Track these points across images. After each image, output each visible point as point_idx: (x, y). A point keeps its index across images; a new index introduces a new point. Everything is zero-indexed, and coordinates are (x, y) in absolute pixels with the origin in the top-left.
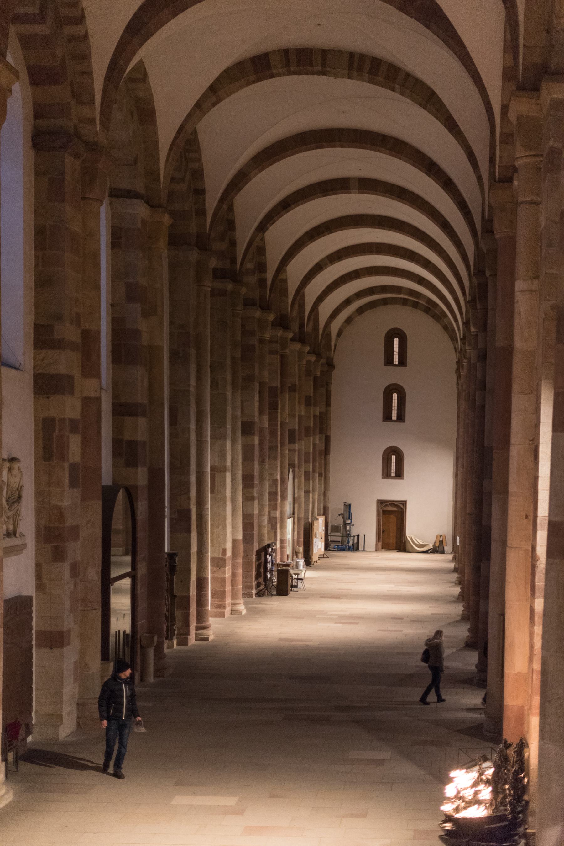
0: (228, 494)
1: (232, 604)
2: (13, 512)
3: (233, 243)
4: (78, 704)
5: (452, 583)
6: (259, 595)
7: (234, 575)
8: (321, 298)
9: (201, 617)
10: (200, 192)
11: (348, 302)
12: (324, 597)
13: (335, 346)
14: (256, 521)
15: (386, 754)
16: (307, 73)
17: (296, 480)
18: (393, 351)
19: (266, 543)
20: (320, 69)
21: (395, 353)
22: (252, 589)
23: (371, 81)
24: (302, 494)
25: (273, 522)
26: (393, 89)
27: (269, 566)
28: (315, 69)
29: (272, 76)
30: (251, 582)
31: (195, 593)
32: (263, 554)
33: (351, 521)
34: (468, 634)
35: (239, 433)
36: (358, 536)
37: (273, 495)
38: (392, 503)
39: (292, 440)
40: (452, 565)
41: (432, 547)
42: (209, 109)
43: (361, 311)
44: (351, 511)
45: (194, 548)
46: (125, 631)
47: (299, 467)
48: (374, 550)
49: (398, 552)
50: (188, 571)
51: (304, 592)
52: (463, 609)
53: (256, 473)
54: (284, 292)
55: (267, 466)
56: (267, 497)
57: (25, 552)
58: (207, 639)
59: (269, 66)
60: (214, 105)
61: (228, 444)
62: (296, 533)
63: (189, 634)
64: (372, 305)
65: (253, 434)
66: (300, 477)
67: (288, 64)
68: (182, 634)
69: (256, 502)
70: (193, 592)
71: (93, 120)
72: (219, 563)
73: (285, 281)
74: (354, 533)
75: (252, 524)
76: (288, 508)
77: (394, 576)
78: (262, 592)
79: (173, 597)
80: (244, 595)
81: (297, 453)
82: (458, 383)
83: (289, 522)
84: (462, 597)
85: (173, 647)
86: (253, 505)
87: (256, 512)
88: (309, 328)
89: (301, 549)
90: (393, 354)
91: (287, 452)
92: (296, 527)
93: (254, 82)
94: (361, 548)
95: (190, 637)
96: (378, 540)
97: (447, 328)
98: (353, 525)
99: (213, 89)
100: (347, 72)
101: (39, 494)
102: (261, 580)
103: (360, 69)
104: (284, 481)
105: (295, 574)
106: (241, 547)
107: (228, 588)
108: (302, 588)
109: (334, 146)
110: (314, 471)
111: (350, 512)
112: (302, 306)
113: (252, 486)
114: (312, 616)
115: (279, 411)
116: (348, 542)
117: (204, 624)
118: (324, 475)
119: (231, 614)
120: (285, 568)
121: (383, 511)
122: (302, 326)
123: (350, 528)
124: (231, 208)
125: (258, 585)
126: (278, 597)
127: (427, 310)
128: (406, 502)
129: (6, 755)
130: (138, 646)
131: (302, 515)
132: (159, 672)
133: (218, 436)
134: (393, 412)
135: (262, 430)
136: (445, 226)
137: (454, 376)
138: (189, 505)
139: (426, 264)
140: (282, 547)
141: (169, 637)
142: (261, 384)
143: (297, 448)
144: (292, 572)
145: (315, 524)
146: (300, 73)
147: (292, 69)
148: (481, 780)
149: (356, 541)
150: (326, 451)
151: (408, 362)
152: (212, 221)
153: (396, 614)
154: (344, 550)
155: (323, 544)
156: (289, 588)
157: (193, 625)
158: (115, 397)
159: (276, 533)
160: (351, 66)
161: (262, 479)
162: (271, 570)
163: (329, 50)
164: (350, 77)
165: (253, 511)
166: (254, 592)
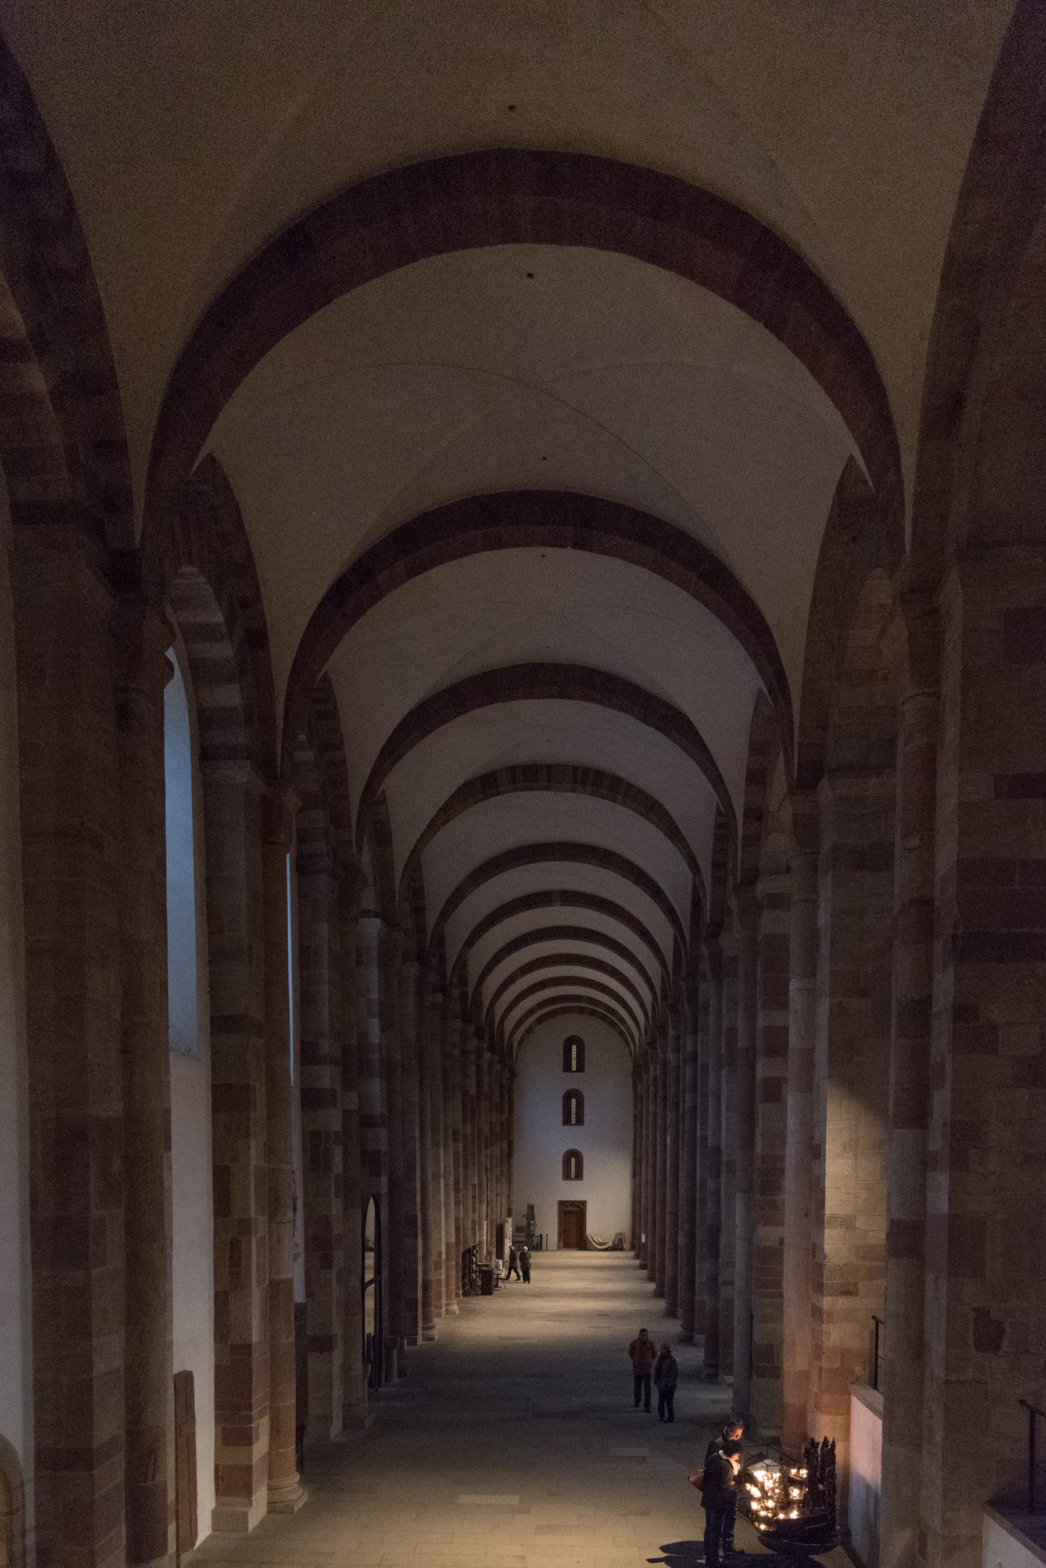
0: (442, 1199)
3: (443, 959)
4: (343, 1406)
6: (465, 1294)
8: (510, 1009)
9: (427, 1318)
11: (531, 1012)
13: (517, 1054)
15: (645, 1452)
19: (471, 1245)
20: (544, 784)
23: (594, 794)
24: (494, 1197)
26: (615, 801)
29: (498, 794)
35: (450, 1141)
36: (541, 1235)
38: (573, 1203)
43: (540, 1020)
47: (491, 1171)
49: (579, 1250)
56: (470, 1201)
58: (433, 1339)
60: (444, 824)
62: (489, 1234)
70: (420, 1295)
72: (438, 1266)
74: (537, 1233)
77: (584, 1273)
82: (635, 1087)
84: (659, 1294)
90: (571, 1061)
91: (483, 1158)
95: (418, 1337)
96: (559, 1240)
98: (536, 1226)
99: (444, 809)
100: (570, 785)
101: (306, 1204)
102: (467, 1281)
106: (453, 1250)
107: (444, 1289)
108: (503, 1287)
114: (522, 1314)
116: (532, 1242)
122: (492, 1036)
123: (534, 1228)
125: (464, 1285)
127: (604, 1018)
130: (383, 1348)
132: (402, 1373)
133: (436, 1144)
134: (572, 1116)
135: (465, 1137)
136: (644, 934)
138: (415, 1209)
139: (613, 972)
142: (465, 1093)
145: (506, 1226)
150: (510, 1156)
151: (586, 1066)
157: (420, 1325)
163: (555, 765)
164: (573, 791)
166: (461, 1292)
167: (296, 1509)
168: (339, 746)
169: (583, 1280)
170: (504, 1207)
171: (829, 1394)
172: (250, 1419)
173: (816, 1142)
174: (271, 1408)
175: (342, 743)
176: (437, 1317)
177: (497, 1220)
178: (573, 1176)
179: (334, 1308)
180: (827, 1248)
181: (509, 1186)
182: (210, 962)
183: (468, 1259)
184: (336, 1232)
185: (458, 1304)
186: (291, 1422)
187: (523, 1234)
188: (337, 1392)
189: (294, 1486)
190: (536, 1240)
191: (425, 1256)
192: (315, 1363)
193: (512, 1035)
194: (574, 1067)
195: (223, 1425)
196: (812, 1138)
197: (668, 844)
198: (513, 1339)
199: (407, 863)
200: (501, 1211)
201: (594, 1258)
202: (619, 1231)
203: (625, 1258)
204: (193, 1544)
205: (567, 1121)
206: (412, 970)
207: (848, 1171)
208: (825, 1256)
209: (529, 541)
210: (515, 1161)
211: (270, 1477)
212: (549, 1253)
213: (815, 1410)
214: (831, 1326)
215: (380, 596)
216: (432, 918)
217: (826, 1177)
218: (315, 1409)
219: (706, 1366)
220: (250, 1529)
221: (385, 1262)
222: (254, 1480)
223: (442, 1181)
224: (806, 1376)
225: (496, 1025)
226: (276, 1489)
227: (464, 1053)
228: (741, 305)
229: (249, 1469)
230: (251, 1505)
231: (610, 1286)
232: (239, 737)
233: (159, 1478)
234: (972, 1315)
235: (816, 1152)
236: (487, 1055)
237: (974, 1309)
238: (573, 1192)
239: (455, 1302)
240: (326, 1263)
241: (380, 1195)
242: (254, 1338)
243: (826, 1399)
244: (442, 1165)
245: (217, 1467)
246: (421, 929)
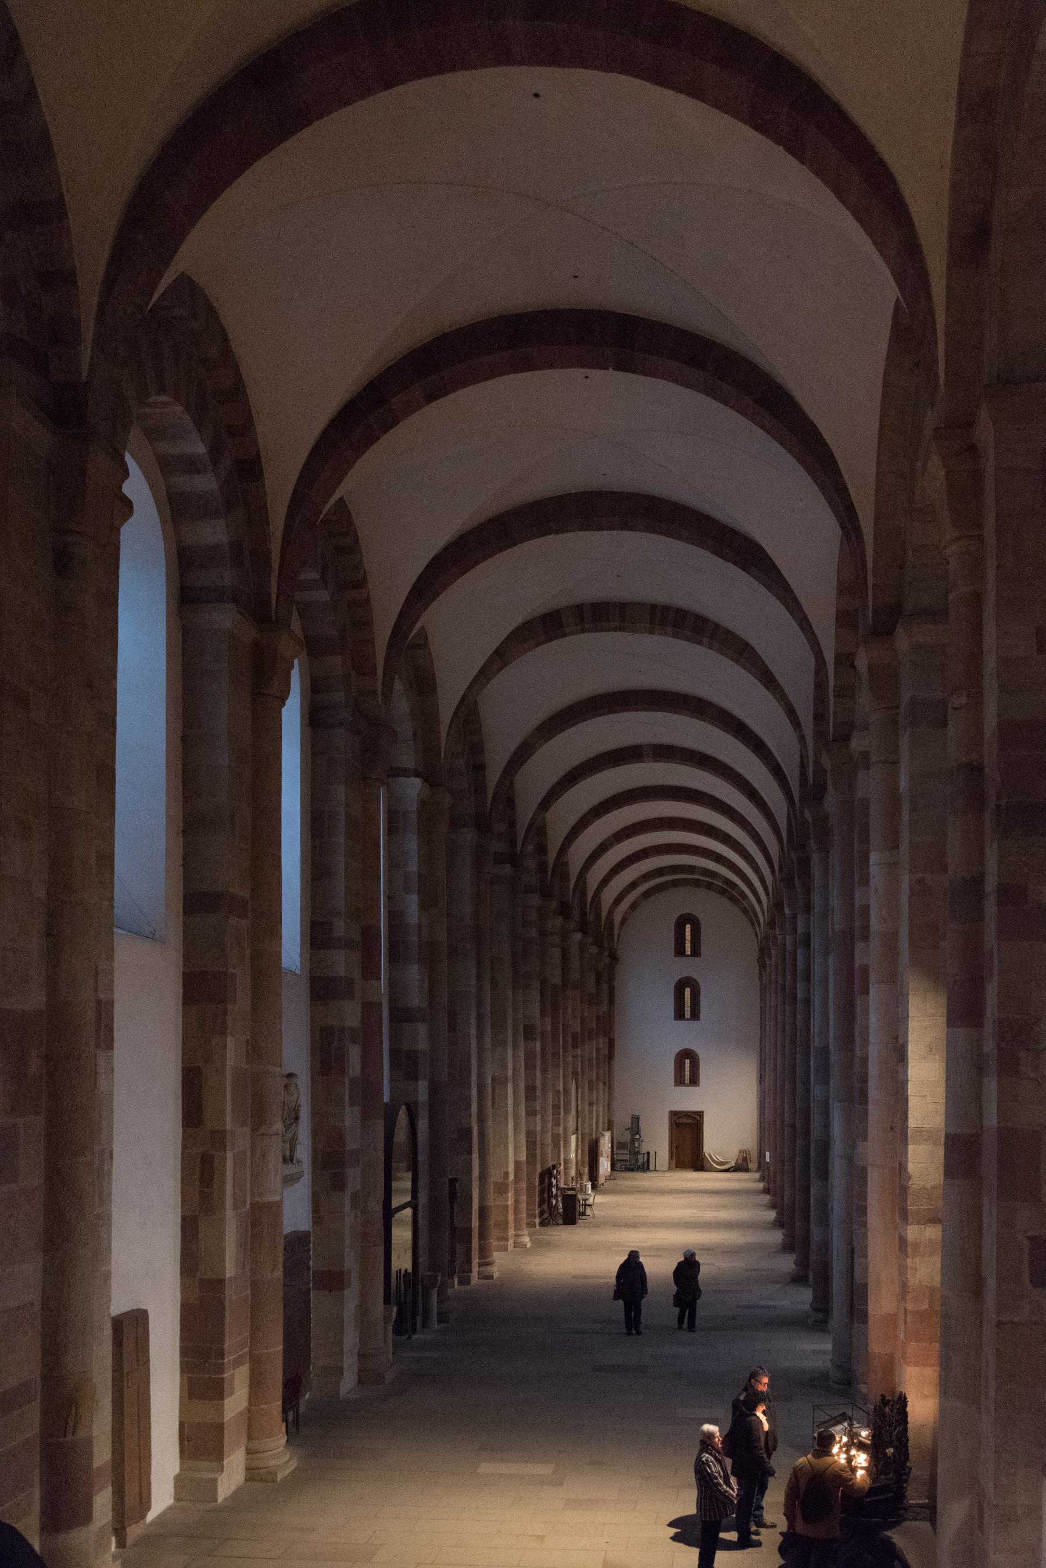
0: (510, 1109)
1: (515, 1236)
2: (290, 1135)
3: (512, 824)
5: (766, 1206)
6: (542, 1224)
7: (517, 1202)
8: (605, 881)
9: (484, 1252)
10: (479, 768)
11: (633, 885)
12: (619, 1226)
14: (538, 1139)
16: (602, 630)
17: (580, 1091)
18: (685, 939)
19: (550, 1164)
20: (617, 624)
21: (686, 942)
22: (535, 1217)
23: (676, 636)
25: (556, 1138)
26: (700, 643)
27: (554, 1190)
29: (564, 635)
30: (535, 1210)
31: (477, 1224)
32: (547, 1176)
33: (640, 1137)
34: (793, 1266)
35: (521, 1039)
36: (648, 1153)
37: (556, 1107)
38: (687, 1114)
39: (575, 1046)
40: (761, 1186)
41: (734, 1165)
42: (494, 675)
43: (647, 895)
44: (640, 1125)
45: (476, 1173)
46: (406, 1270)
47: (583, 1073)
48: (667, 1169)
49: (694, 1171)
50: (470, 1198)
51: (593, 1220)
52: (783, 1237)
53: (538, 1084)
54: (565, 877)
55: (550, 1076)
56: (550, 1111)
57: (301, 1181)
58: (492, 1277)
60: (500, 670)
61: (510, 1051)
62: (579, 1151)
63: (471, 1272)
65: (535, 1039)
66: (583, 1087)
68: (464, 1272)
69: (539, 1117)
70: (475, 1224)
71: (375, 692)
72: (502, 1189)
73: (566, 864)
74: (644, 1150)
75: (534, 1143)
76: (571, 1123)
77: (694, 1199)
78: (546, 1221)
79: (454, 1229)
80: (531, 1225)
81: (579, 1059)
82: (761, 975)
83: (573, 1138)
84: (779, 1224)
85: (454, 1287)
86: (535, 1121)
87: (539, 1128)
88: (591, 917)
89: (586, 1170)
91: (570, 1058)
92: (580, 1143)
93: (543, 643)
94: (652, 1167)
96: (671, 1158)
97: (747, 912)
98: (643, 1141)
101: (317, 1114)
102: (545, 1207)
104: (566, 1092)
105: (584, 1200)
107: (511, 1217)
108: (591, 1215)
109: (629, 710)
110: (597, 1079)
111: (638, 1126)
112: (583, 893)
113: (534, 1099)
115: (561, 1011)
117: (488, 1260)
118: (609, 1085)
119: (515, 1247)
120: (569, 1193)
121: (676, 1123)
122: (583, 915)
124: (511, 786)
125: (541, 1213)
126: (566, 1226)
127: (723, 892)
128: (702, 1112)
129: (287, 1415)
130: (420, 1287)
131: (587, 1131)
135: (543, 1034)
136: (753, 795)
137: (756, 966)
140: (566, 1168)
141: (451, 1276)
142: (543, 982)
143: (579, 1053)
144: (580, 1197)
145: (602, 1141)
147: (587, 626)
148: (853, 1444)
149: (645, 1160)
150: (611, 1056)
152: (494, 799)
153: (703, 1245)
154: (631, 1170)
155: (609, 1163)
156: (577, 1217)
157: (475, 1261)
158: (392, 1001)
159: (559, 1152)
160: (652, 621)
161: (544, 1091)
162: (556, 1195)
164: (651, 632)
165: (535, 1127)
166: (537, 1221)
167: (280, 1477)
168: (361, 583)
169: (691, 1207)
170: (601, 1119)
171: (915, 1342)
172: (221, 1368)
173: (901, 1042)
174: (251, 1355)
175: (365, 579)
176: (498, 1250)
177: (591, 1135)
178: (687, 1081)
179: (347, 1237)
180: (911, 1167)
181: (610, 1094)
182: (183, 831)
183: (547, 1180)
184: (348, 1148)
185: (529, 1235)
186: (276, 1375)
187: (627, 1152)
188: (351, 1338)
189: (279, 1450)
190: (641, 1159)
191: (483, 1176)
192: (319, 1303)
193: (611, 912)
194: (688, 951)
195: (190, 1375)
196: (897, 1038)
197: (762, 693)
198: (586, 1277)
199: (455, 715)
200: (597, 1123)
201: (708, 1180)
202: (744, 1148)
203: (746, 1180)
204: (143, 1516)
205: (679, 1015)
206: (468, 836)
207: (935, 1077)
208: (909, 1178)
209: (566, 363)
210: (616, 1062)
211: (250, 1438)
212: (656, 1174)
213: (902, 1361)
214: (917, 1260)
215: (396, 421)
216: (493, 776)
217: (909, 1083)
218: (319, 1358)
219: (815, 1310)
220: (220, 1500)
221: (423, 1182)
222: (226, 1439)
223: (510, 1088)
224: (891, 1320)
225: (589, 900)
226: (256, 1452)
227: (542, 933)
228: (756, 127)
229: (220, 1428)
230: (222, 1471)
231: (724, 1215)
232: (226, 577)
233: (82, 1433)
234: (1026, 1243)
235: (900, 1054)
236: (578, 937)
237: (1028, 1238)
238: (688, 1100)
239: (526, 1232)
240: (338, 1184)
241: (416, 1103)
242: (227, 1271)
243: (912, 1347)
244: (510, 1067)
245: (182, 1425)
246: (480, 789)
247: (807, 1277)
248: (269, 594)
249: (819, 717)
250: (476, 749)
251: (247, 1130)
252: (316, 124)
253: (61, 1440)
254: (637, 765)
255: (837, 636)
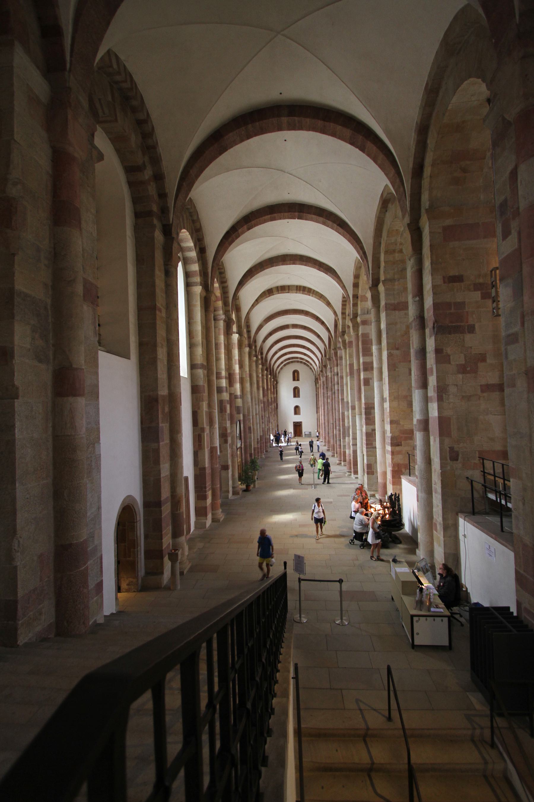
3: (256, 347)
11: (282, 363)
20: (288, 291)
28: (286, 291)
29: (273, 295)
38: (298, 422)
42: (255, 306)
43: (285, 365)
59: (273, 292)
60: (256, 305)
64: (288, 363)
67: (278, 291)
93: (268, 297)
99: (257, 300)
100: (295, 291)
103: (300, 290)
122: (270, 371)
127: (305, 364)
139: (308, 349)
146: (281, 293)
160: (297, 290)
164: (296, 293)
168: (225, 282)
179: (229, 455)
188: (230, 483)
193: (276, 370)
215: (239, 236)
230: (207, 519)
233: (181, 510)
240: (226, 441)
241: (240, 420)
247: (341, 463)
248: (208, 284)
249: (343, 313)
250: (248, 327)
251: (208, 427)
252: (229, 151)
253: (176, 512)
254: (287, 330)
255: (353, 290)
